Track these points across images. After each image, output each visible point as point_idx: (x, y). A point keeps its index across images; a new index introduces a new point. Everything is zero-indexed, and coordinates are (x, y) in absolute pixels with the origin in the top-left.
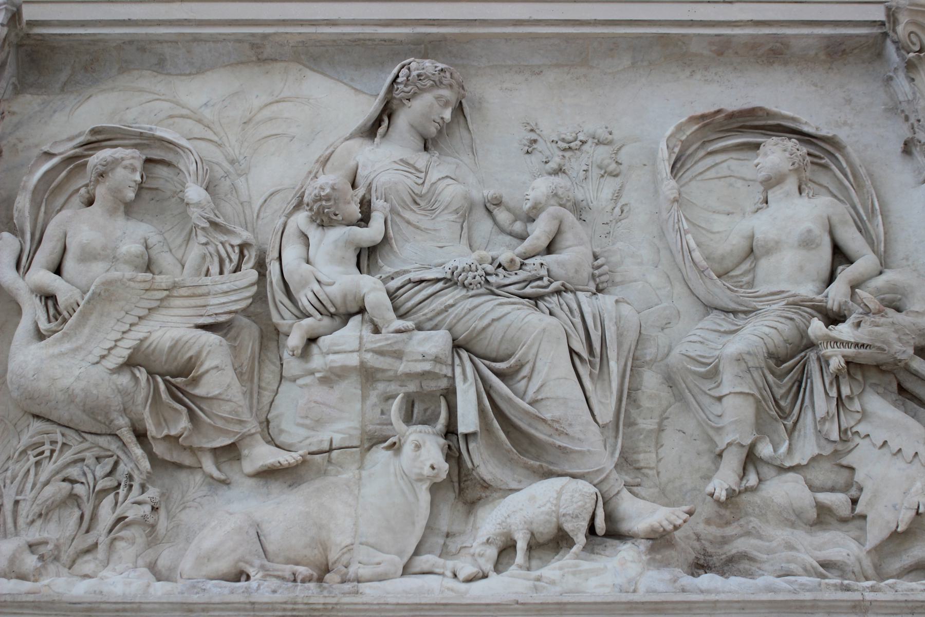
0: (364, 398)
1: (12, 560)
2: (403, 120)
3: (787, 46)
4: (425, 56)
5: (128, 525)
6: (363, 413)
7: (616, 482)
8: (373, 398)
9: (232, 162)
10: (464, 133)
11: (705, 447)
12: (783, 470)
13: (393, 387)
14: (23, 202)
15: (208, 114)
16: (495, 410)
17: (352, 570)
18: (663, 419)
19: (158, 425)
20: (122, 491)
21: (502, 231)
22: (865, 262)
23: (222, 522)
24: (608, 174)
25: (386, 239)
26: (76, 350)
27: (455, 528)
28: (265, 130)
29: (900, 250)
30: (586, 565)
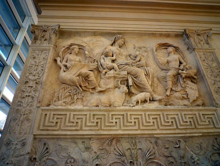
0: (114, 81)
1: (61, 104)
2: (116, 43)
3: (170, 35)
4: (120, 35)
5: (79, 99)
6: (114, 83)
7: (153, 93)
8: (115, 81)
9: (91, 49)
11: (164, 89)
12: (176, 91)
13: (118, 79)
14: (61, 53)
15: (87, 43)
16: (134, 83)
17: (115, 105)
18: (158, 85)
19: (83, 84)
20: (78, 94)
21: (132, 59)
22: (184, 64)
23: (94, 99)
24: (146, 52)
25: (116, 59)
27: (129, 100)
28: (96, 45)
29: (188, 62)
30: (150, 104)
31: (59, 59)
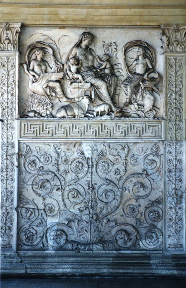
8: (80, 91)
10: (94, 44)
20: (47, 104)
26: (39, 84)
31: (25, 66)
